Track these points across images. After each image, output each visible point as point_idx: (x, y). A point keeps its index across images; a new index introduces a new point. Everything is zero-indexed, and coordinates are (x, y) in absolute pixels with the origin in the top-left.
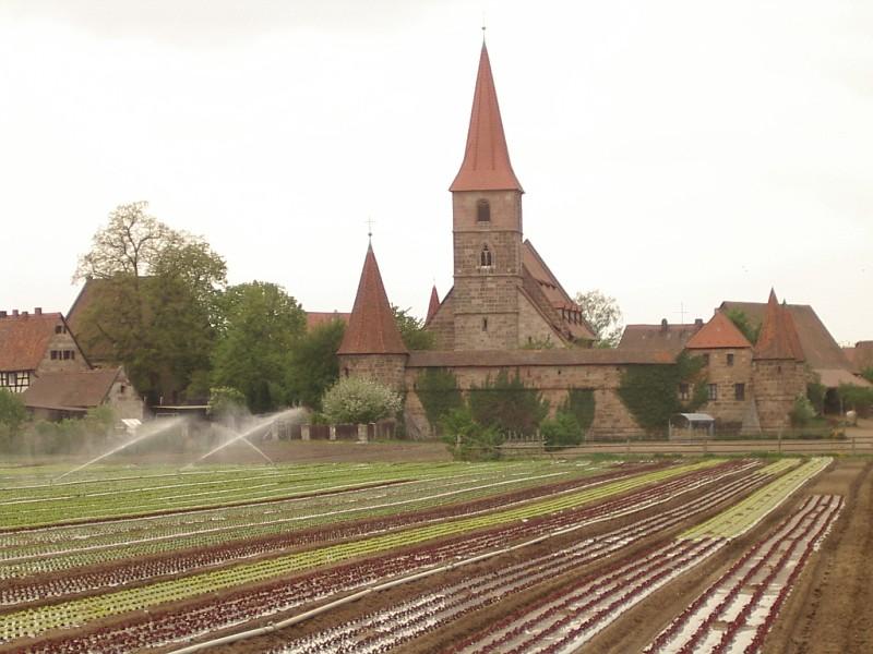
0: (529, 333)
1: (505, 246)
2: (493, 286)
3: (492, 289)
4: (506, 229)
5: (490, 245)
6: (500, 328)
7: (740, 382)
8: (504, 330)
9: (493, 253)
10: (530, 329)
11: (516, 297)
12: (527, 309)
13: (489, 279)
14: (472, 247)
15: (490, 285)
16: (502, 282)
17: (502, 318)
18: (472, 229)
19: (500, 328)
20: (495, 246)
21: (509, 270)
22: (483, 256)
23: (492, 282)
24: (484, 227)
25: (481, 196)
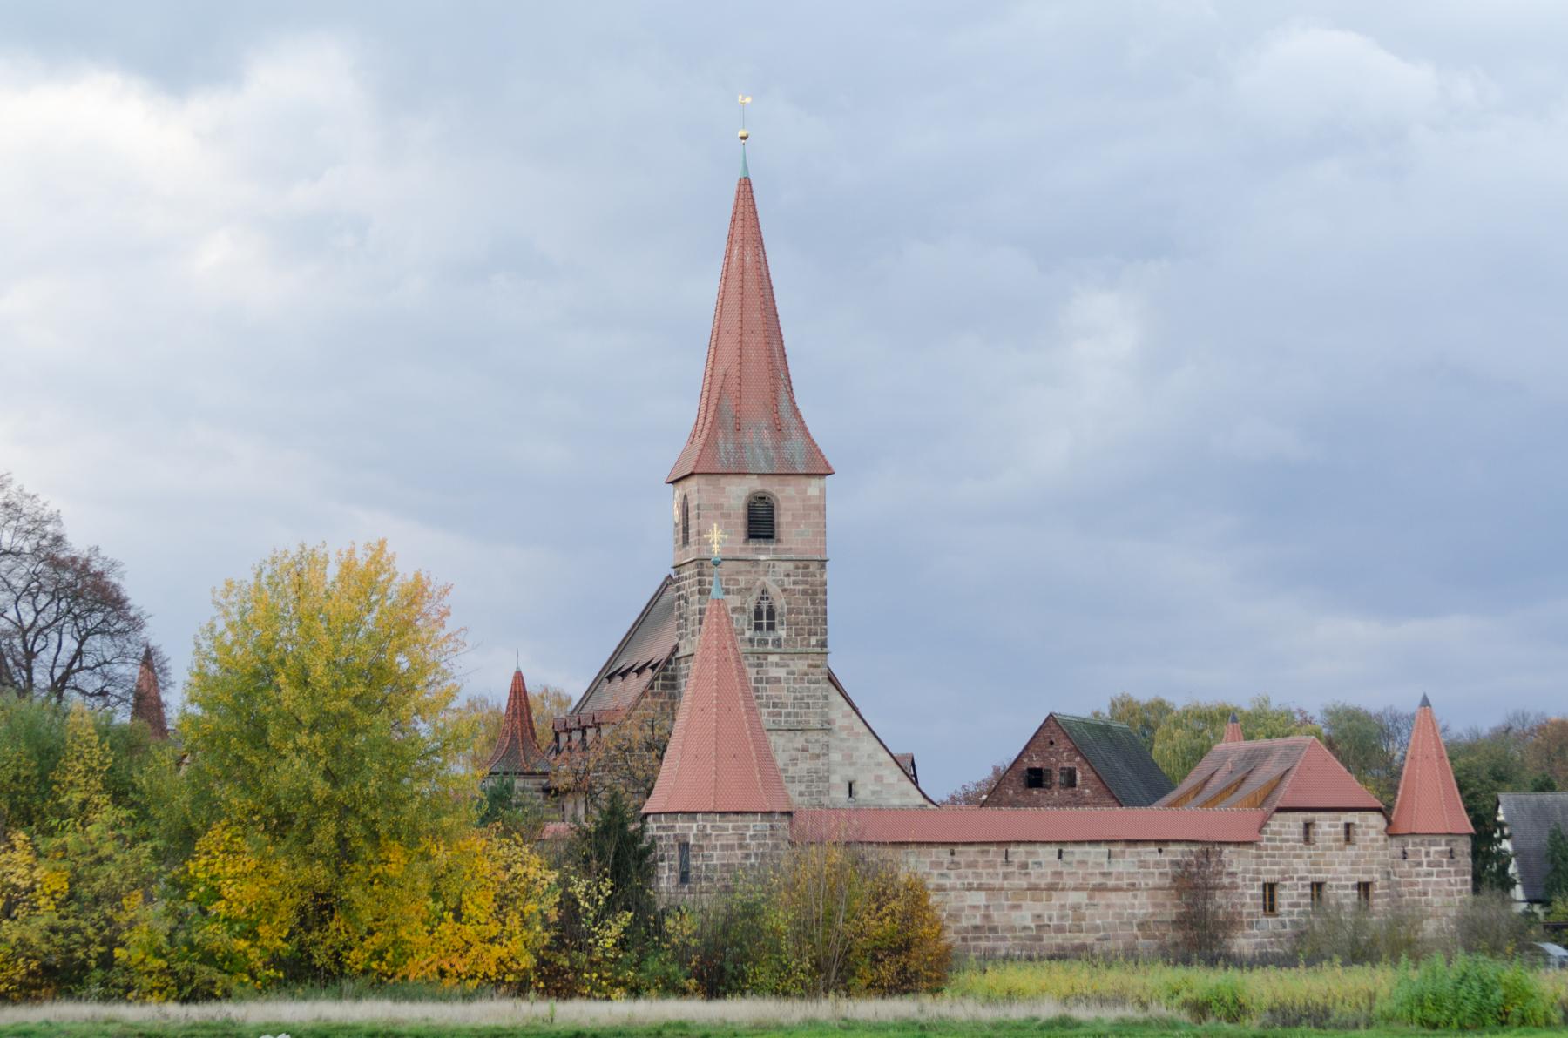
0: (850, 773)
1: (805, 592)
2: (781, 673)
3: (778, 680)
4: (807, 556)
5: (774, 590)
6: (794, 761)
7: (1366, 878)
8: (804, 766)
9: (780, 603)
10: (852, 764)
11: (826, 697)
12: (846, 722)
13: (772, 658)
14: (739, 592)
15: (775, 672)
16: (800, 665)
17: (799, 740)
18: (739, 555)
19: (794, 761)
20: (784, 590)
21: (813, 641)
22: (758, 614)
23: (777, 665)
24: (763, 553)
25: (753, 485)
